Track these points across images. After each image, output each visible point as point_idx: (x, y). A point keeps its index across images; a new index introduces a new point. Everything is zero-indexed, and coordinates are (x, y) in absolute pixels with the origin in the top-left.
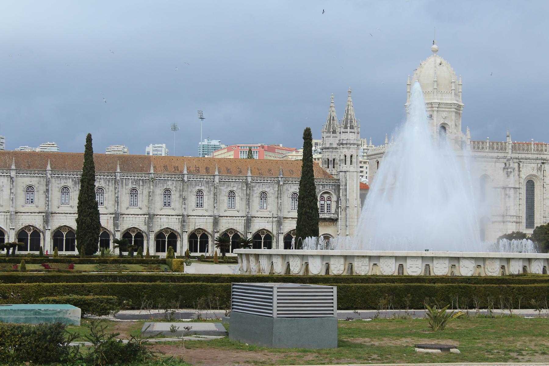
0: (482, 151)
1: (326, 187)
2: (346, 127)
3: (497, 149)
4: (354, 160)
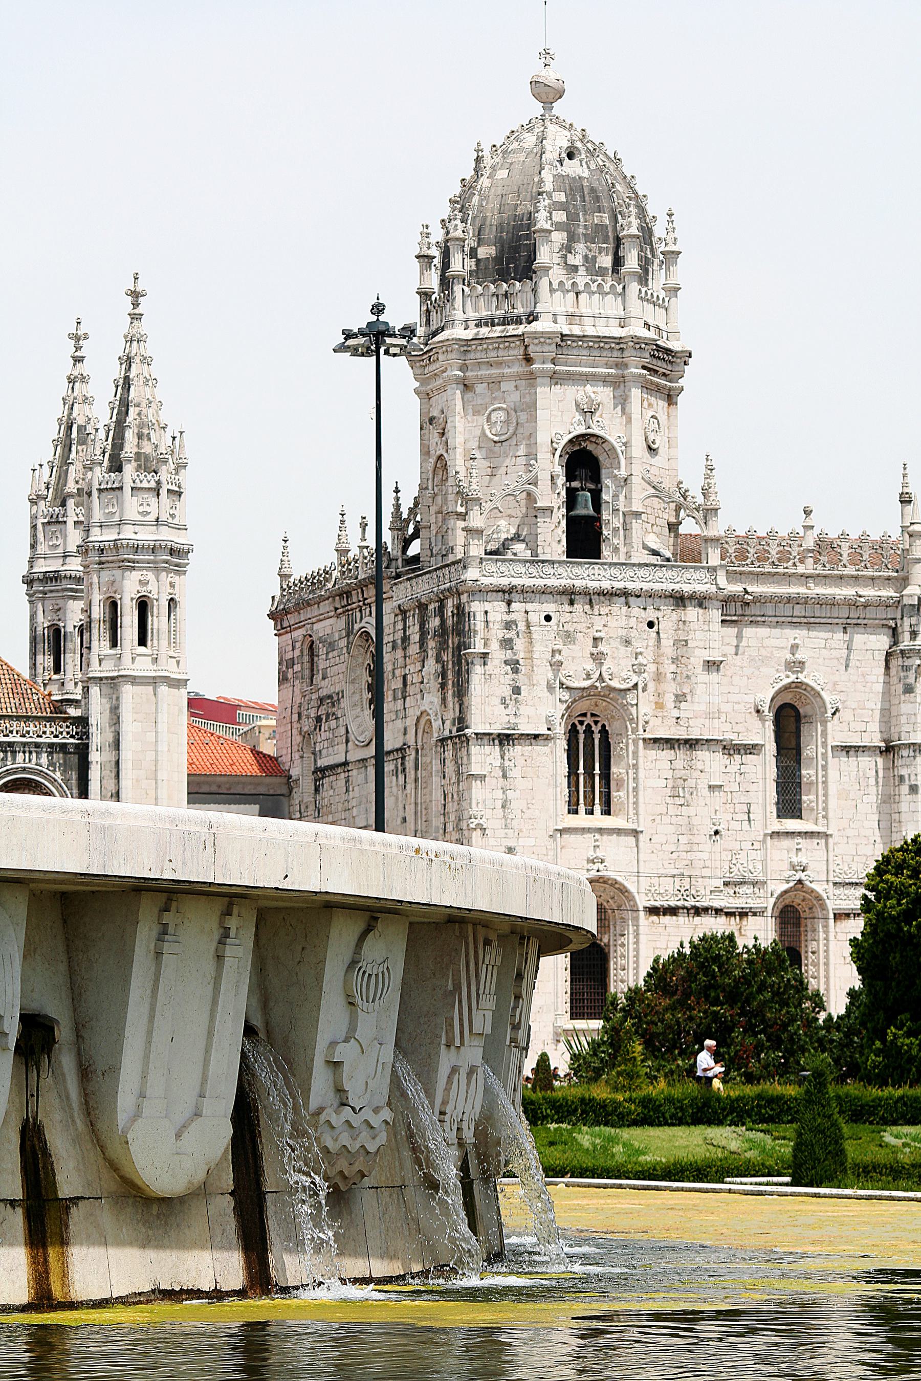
0: (781, 570)
1: (20, 757)
2: (116, 466)
3: (856, 557)
4: (157, 621)
